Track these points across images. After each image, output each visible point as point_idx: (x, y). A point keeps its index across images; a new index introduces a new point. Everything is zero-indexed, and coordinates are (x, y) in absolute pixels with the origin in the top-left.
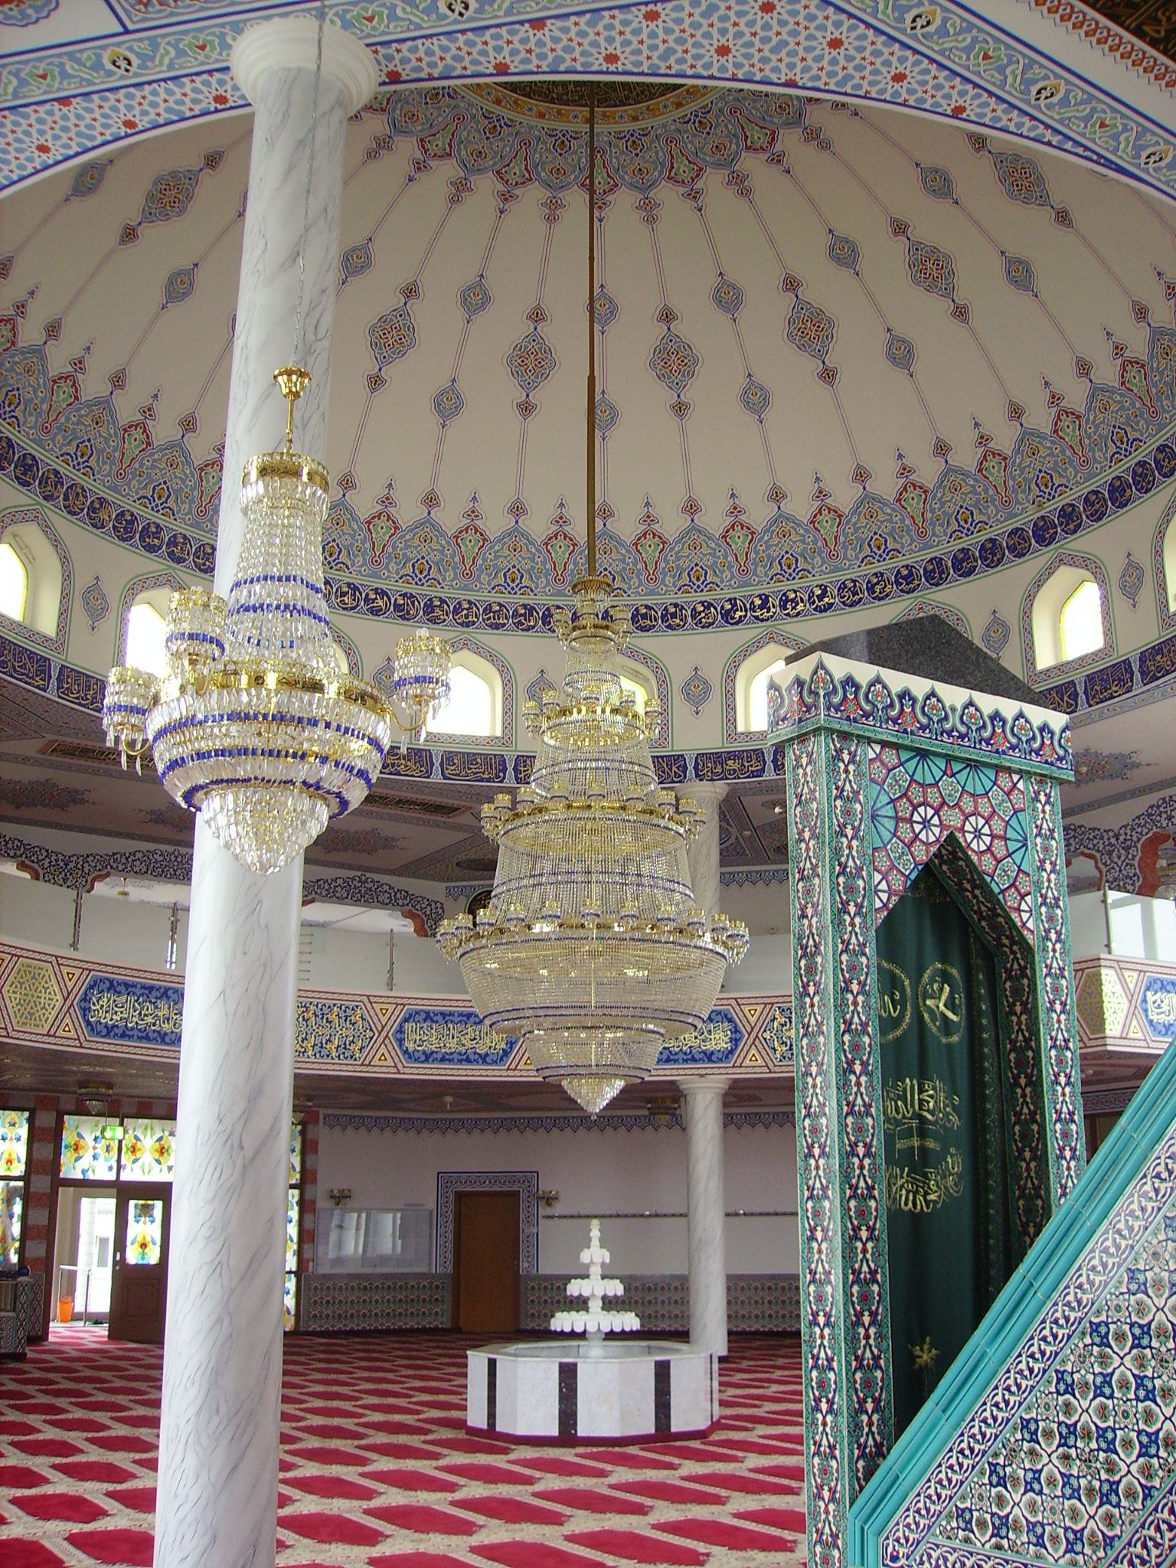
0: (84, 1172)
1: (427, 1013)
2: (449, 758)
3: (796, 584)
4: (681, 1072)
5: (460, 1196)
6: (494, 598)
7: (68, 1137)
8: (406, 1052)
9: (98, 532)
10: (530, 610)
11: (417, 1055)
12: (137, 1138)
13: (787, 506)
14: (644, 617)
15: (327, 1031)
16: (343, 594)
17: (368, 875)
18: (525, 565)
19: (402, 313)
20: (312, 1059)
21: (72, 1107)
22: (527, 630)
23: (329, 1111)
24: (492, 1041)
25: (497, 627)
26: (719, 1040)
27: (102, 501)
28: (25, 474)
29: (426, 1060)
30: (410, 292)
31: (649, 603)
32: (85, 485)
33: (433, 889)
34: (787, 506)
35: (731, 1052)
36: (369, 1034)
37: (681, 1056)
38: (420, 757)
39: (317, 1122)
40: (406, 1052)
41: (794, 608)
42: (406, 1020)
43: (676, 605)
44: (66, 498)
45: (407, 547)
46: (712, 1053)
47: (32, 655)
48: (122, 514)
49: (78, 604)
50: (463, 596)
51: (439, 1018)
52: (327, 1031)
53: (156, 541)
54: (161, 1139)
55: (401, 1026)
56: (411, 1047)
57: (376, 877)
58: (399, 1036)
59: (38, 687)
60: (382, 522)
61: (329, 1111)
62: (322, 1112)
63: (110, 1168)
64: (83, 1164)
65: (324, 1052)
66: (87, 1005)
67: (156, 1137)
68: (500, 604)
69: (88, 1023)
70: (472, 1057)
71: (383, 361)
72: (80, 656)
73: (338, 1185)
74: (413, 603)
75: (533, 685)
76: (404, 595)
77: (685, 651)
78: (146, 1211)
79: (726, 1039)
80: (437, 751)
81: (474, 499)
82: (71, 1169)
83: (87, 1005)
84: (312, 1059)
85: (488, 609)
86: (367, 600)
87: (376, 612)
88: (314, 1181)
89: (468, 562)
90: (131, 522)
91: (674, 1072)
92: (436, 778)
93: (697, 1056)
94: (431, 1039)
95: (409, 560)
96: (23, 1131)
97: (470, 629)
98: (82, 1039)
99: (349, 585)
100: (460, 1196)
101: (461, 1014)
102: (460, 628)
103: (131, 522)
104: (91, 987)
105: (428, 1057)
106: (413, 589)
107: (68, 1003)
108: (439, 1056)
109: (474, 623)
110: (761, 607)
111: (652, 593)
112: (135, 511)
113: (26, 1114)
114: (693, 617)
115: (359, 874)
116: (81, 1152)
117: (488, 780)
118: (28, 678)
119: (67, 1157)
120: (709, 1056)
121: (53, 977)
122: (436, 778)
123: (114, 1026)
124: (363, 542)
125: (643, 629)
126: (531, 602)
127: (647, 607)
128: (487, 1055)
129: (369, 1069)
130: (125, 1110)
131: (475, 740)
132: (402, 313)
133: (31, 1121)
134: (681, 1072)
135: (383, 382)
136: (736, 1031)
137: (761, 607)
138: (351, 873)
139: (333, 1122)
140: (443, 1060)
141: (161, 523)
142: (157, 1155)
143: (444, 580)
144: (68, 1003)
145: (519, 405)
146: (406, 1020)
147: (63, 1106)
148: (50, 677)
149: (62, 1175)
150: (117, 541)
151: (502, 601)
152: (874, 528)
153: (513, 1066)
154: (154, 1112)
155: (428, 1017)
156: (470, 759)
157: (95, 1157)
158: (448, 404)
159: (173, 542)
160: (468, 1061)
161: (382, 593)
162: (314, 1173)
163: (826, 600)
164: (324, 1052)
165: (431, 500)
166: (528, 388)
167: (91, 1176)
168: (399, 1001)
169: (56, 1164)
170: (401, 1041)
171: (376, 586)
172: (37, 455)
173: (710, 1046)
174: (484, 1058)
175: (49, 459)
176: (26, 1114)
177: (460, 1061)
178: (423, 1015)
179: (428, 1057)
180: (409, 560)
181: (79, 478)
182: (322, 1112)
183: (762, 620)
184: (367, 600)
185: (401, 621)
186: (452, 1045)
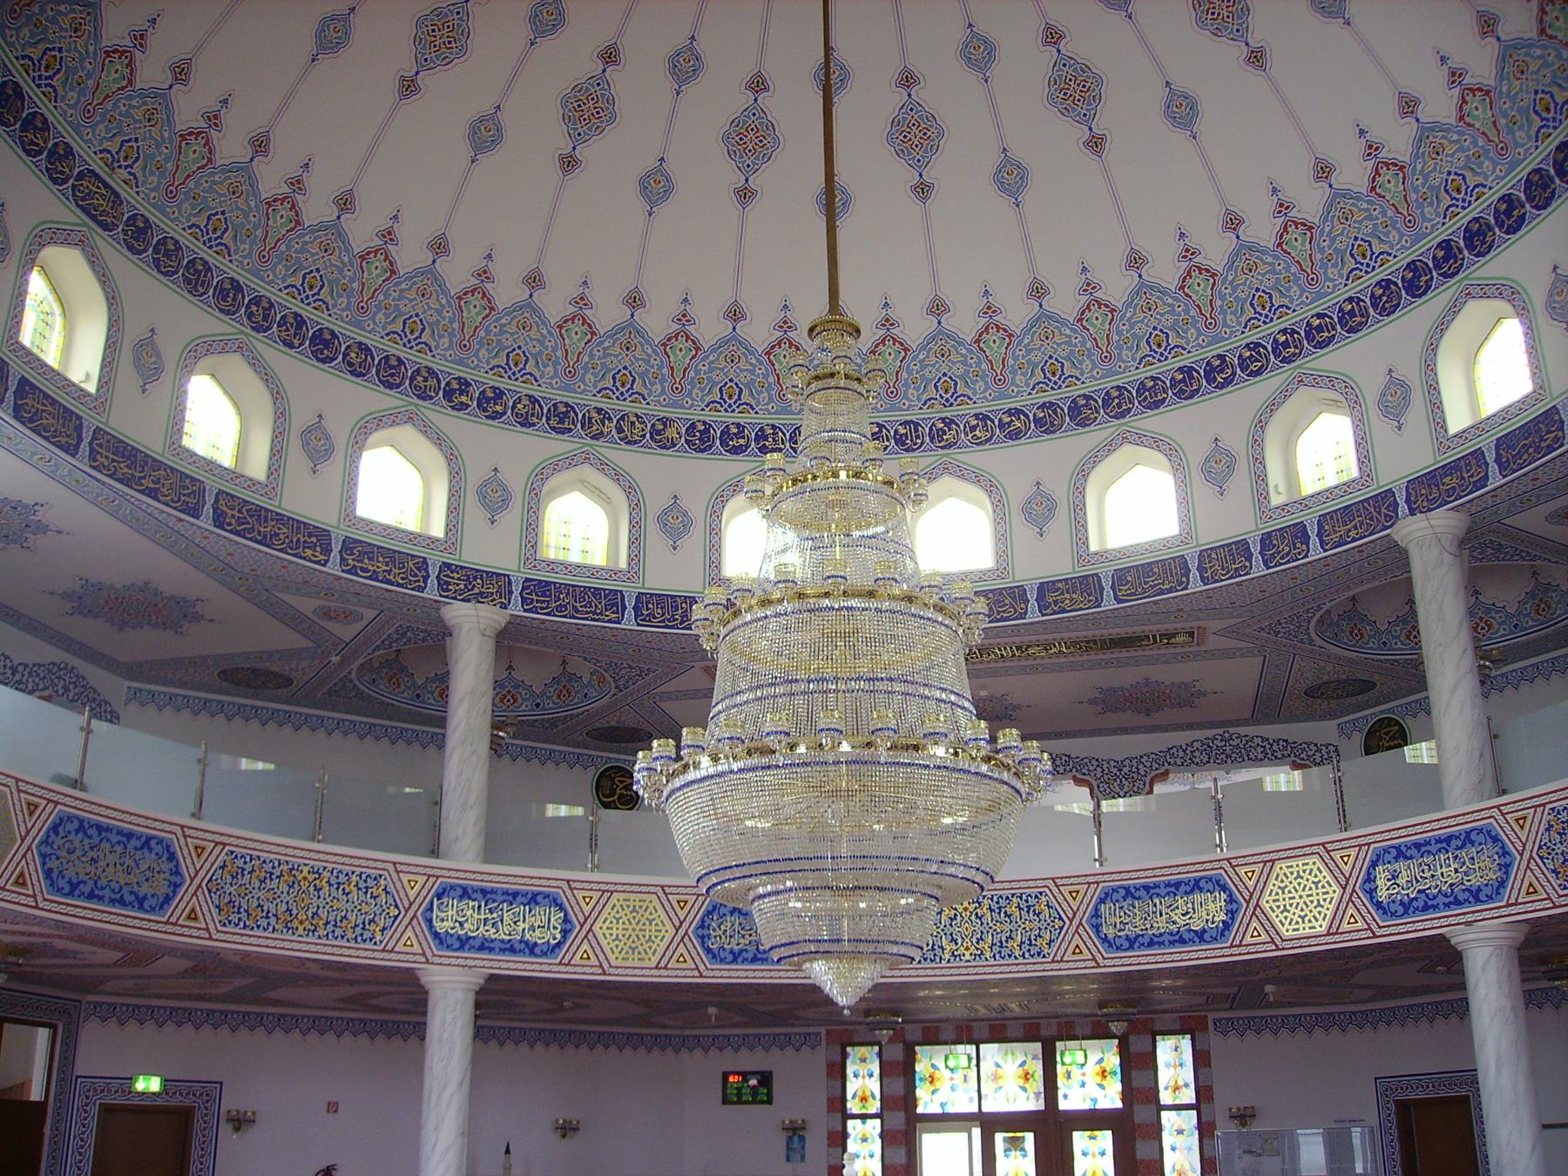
0: (942, 1105)
1: (1127, 889)
2: (1120, 577)
3: (1474, 211)
4: (1444, 922)
5: (1403, 1108)
6: (1144, 373)
7: (921, 1067)
8: (1105, 940)
9: (669, 452)
10: (1188, 371)
11: (1118, 941)
12: (998, 1065)
13: (1425, 114)
14: (1319, 329)
15: (1007, 927)
16: (973, 429)
17: (1232, 730)
18: (1168, 321)
19: (911, 106)
20: (992, 962)
21: (918, 1036)
22: (1191, 397)
23: (1218, 1015)
24: (1211, 909)
25: (1156, 405)
26: (1483, 870)
27: (665, 422)
28: (561, 421)
29: (1131, 947)
30: (907, 80)
31: (1318, 310)
32: (639, 412)
33: (1323, 731)
34: (1425, 114)
35: (1502, 883)
36: (1058, 923)
37: (1441, 899)
38: (1087, 586)
39: (1206, 1029)
40: (1105, 940)
41: (1483, 243)
42: (1102, 901)
43: (1350, 300)
44: (620, 430)
45: (1029, 352)
46: (1479, 890)
47: (597, 592)
48: (693, 426)
49: (652, 528)
50: (1109, 383)
51: (1142, 893)
52: (1007, 927)
53: (742, 441)
54: (1024, 1063)
55: (1096, 909)
56: (1110, 932)
57: (1243, 730)
58: (1094, 921)
59: (610, 621)
60: (993, 335)
61: (1218, 1015)
62: (1211, 1016)
63: (971, 1100)
64: (938, 1098)
65: (1005, 952)
66: (705, 932)
67: (1019, 1061)
68: (1153, 378)
69: (708, 951)
70: (1186, 936)
71: (748, 170)
72: (664, 577)
73: (1240, 1102)
74: (1055, 412)
75: (1207, 460)
76: (1042, 407)
77: (1365, 355)
78: (1015, 1144)
79: (1495, 867)
80: (1106, 571)
81: (1084, 269)
82: (927, 1102)
83: (705, 932)
84: (992, 962)
85: (1142, 388)
86: (1001, 425)
87: (1015, 435)
88: (1210, 1099)
89: (1103, 343)
90: (707, 431)
91: (1436, 923)
92: (1109, 604)
93: (1461, 897)
94: (1136, 919)
95: (1035, 365)
96: (875, 1067)
97: (1127, 419)
98: (702, 968)
99: (976, 416)
100: (1403, 1108)
101: (1168, 885)
102: (1116, 422)
103: (707, 431)
104: (709, 913)
105: (1132, 942)
106: (1051, 396)
107: (681, 932)
108: (1146, 940)
109: (1129, 410)
110: (1446, 259)
111: (1320, 296)
112: (707, 419)
113: (876, 1048)
114: (1374, 306)
115: (1220, 731)
116: (937, 1084)
117: (1170, 591)
118: (596, 615)
119: (922, 1092)
120: (1475, 895)
121: (659, 907)
122: (1109, 604)
123: (741, 951)
124: (979, 364)
125: (1321, 345)
126: (1186, 363)
127: (1319, 316)
128: (1204, 931)
129: (1062, 965)
130: (976, 1036)
131: (1151, 547)
132: (911, 106)
133: (880, 1055)
134: (1444, 922)
135: (930, 186)
136: (1505, 853)
137: (1446, 259)
138: (1210, 733)
139: (1224, 1027)
140: (1151, 944)
141: (742, 422)
142: (1021, 1082)
143: (1082, 374)
144: (681, 932)
145: (1087, 144)
146: (1102, 901)
147: (909, 1038)
148: (624, 608)
149: (920, 1110)
150: (694, 454)
151: (1153, 373)
152: (1532, 85)
153: (1237, 942)
154: (943, 1037)
155: (1129, 893)
156: (1146, 569)
157: (953, 1089)
158: (1011, 178)
159: (760, 436)
160: (1182, 941)
161: (1018, 412)
162: (1209, 1089)
163: (1515, 213)
164: (1005, 952)
165: (1038, 291)
166: (1087, 119)
167: (950, 1109)
168: (1091, 879)
169: (909, 1100)
170: (1097, 928)
171: (1007, 407)
172: (570, 401)
173: (1475, 881)
174: (1201, 936)
175: (585, 399)
176: (876, 1048)
177: (1172, 943)
178: (1123, 892)
179: (1132, 942)
180: (1035, 365)
181: (628, 407)
182: (1211, 1016)
183: (1452, 275)
184: (1001, 425)
185: (1047, 437)
186: (1161, 925)
